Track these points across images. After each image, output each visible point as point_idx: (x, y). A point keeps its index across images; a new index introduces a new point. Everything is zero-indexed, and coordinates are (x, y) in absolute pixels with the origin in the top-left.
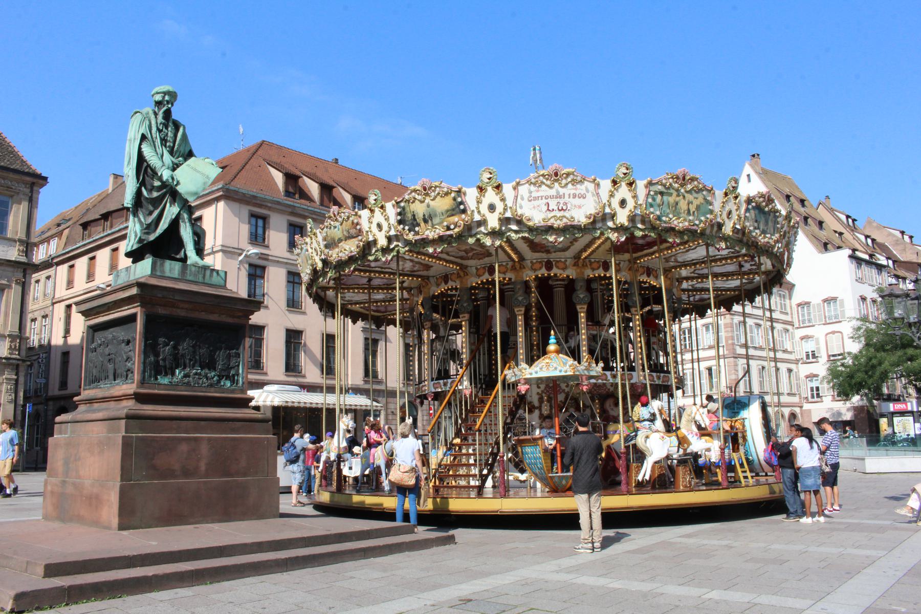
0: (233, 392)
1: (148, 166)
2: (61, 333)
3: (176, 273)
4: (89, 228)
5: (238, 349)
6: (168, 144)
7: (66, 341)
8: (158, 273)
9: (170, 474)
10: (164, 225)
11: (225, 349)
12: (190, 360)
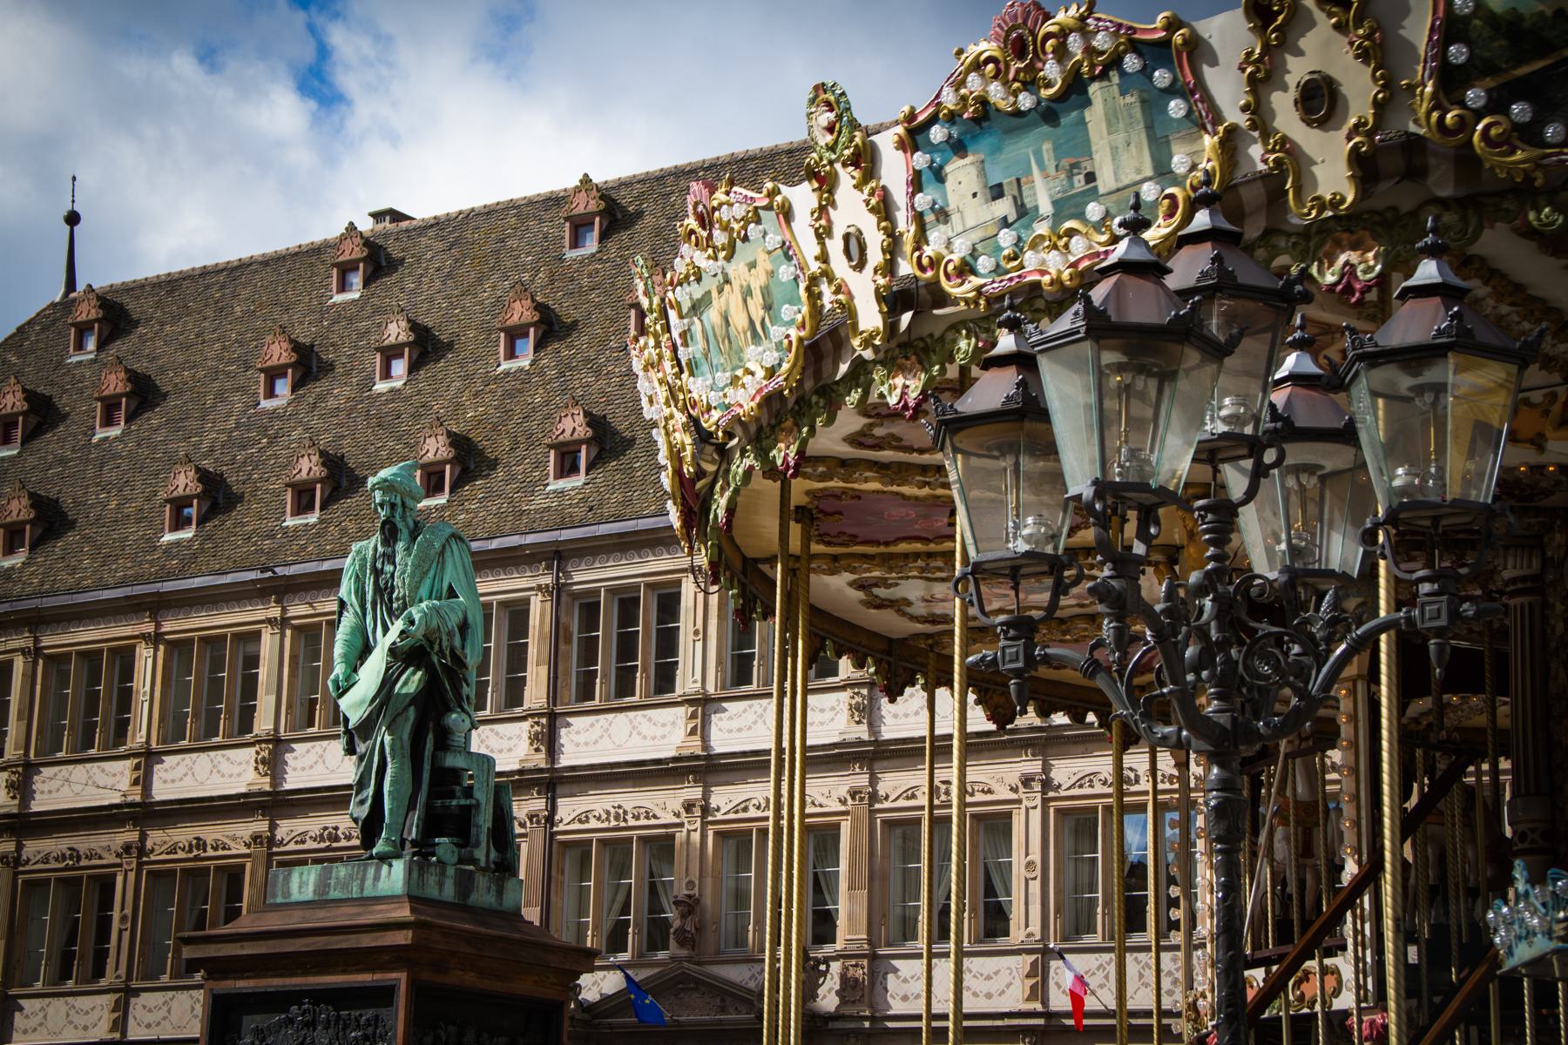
8: (279, 900)
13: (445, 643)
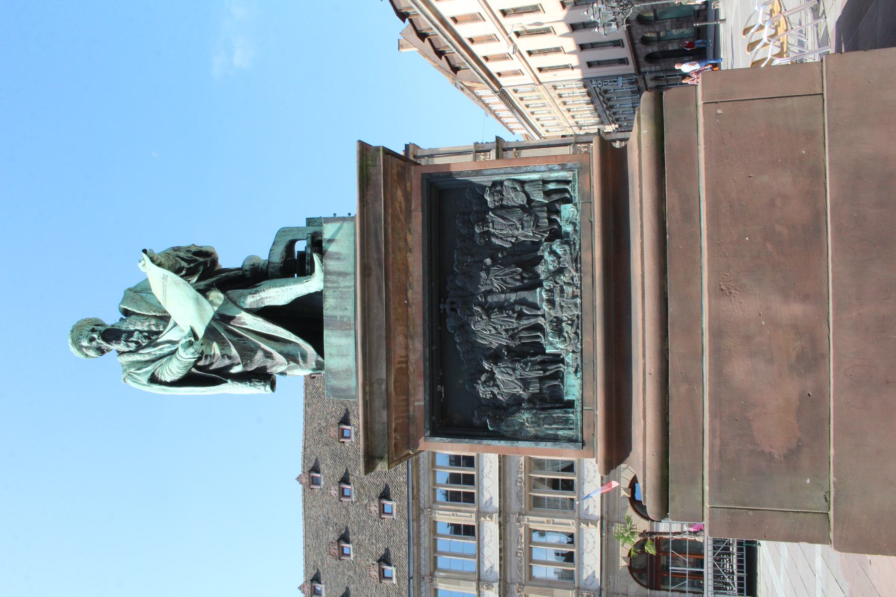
0: (587, 199)
1: (195, 365)
2: (569, 71)
4: (457, 65)
5: (483, 188)
6: (154, 329)
7: (577, 67)
9: (811, 407)
11: (484, 222)
12: (521, 316)
13: (182, 254)
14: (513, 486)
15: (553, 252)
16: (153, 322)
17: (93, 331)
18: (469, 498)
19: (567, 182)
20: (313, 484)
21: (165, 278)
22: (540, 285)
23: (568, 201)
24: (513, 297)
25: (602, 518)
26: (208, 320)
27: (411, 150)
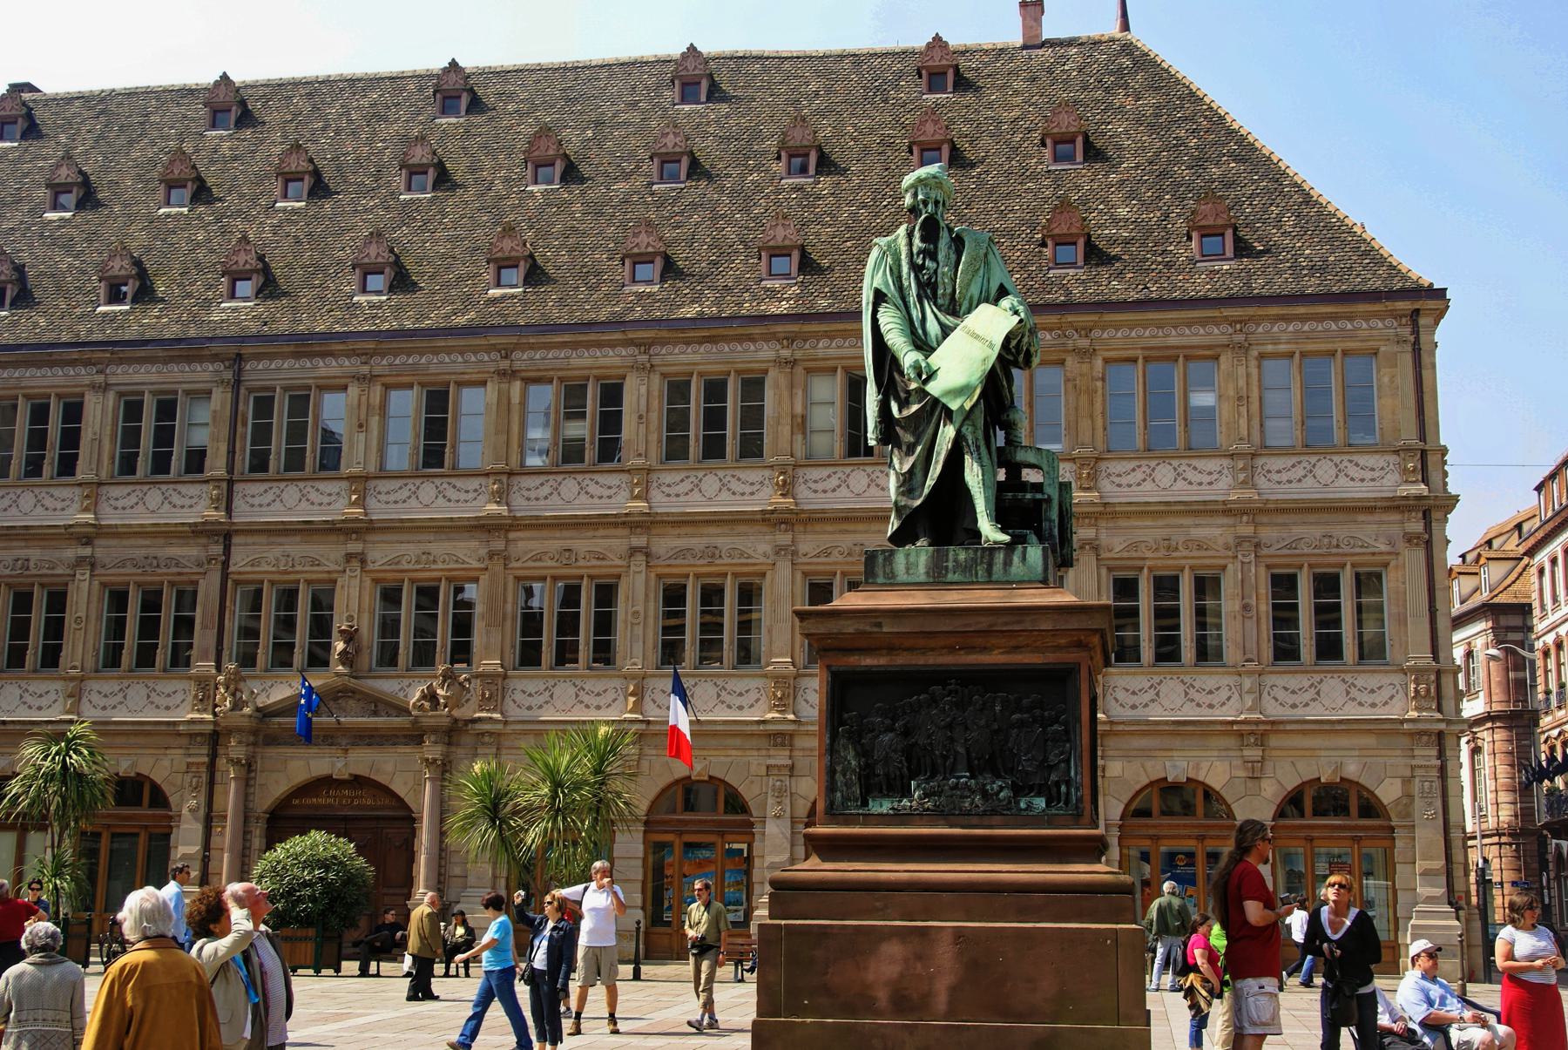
3: (921, 573)
6: (940, 292)
10: (936, 470)
13: (1026, 340)
14: (705, 541)
15: (1001, 789)
16: (949, 291)
17: (936, 203)
18: (675, 450)
19: (1067, 803)
20: (684, 85)
21: (991, 346)
22: (972, 777)
23: (1048, 805)
24: (961, 750)
25: (648, 722)
26: (944, 400)
27: (1431, 304)
